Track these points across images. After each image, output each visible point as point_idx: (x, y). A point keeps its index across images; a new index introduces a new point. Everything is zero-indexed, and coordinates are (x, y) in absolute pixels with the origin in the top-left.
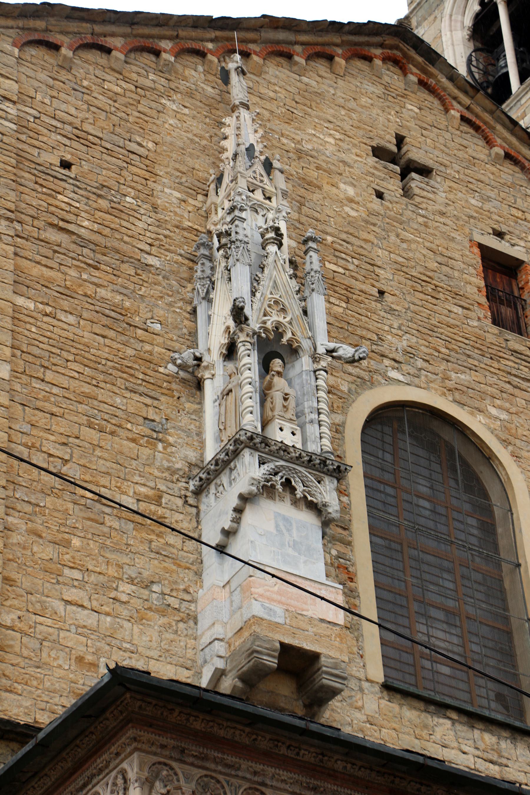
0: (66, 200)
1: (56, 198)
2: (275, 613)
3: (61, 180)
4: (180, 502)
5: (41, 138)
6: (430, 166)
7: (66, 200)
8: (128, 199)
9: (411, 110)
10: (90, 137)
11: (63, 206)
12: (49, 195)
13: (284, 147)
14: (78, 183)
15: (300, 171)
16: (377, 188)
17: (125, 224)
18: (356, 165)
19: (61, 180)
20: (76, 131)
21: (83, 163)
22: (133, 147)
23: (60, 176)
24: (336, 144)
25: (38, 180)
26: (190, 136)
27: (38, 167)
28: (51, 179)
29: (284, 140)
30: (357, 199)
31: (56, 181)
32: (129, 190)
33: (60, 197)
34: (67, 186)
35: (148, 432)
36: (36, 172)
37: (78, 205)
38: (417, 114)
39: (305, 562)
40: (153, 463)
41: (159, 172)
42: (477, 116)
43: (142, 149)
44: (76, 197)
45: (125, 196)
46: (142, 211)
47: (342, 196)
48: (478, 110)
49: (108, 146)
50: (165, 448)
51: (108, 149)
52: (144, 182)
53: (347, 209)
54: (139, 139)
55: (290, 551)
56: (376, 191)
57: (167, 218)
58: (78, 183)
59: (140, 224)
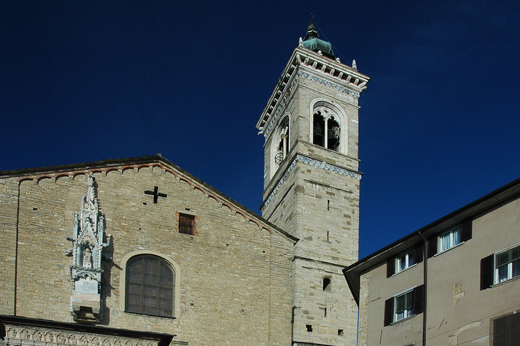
0: (35, 218)
1: (32, 218)
2: (79, 301)
3: (34, 213)
4: (67, 281)
5: (27, 204)
6: (166, 194)
7: (35, 218)
8: (55, 215)
9: (163, 179)
10: (43, 201)
11: (34, 219)
12: (30, 217)
13: (112, 195)
14: (39, 213)
15: (117, 201)
16: (144, 202)
17: (54, 221)
18: (137, 197)
19: (34, 213)
20: (38, 200)
21: (41, 208)
22: (58, 202)
23: (33, 212)
24: (131, 192)
25: (26, 214)
26: (78, 196)
27: (26, 211)
28: (30, 213)
29: (112, 193)
30: (136, 206)
31: (32, 214)
32: (56, 213)
33: (33, 217)
34: (35, 214)
35: (58, 268)
36: (25, 212)
37: (39, 219)
38: (164, 180)
39: (92, 291)
40: (60, 274)
41: (66, 207)
42: (186, 178)
43: (61, 202)
44: (38, 217)
45: (54, 214)
46: (60, 218)
47: (131, 205)
48: (186, 176)
49: (49, 203)
50: (63, 271)
51: (49, 203)
52: (61, 210)
53: (131, 209)
54: (60, 200)
55: (88, 289)
56: (144, 203)
57: (68, 218)
58: (39, 213)
59: (59, 221)
